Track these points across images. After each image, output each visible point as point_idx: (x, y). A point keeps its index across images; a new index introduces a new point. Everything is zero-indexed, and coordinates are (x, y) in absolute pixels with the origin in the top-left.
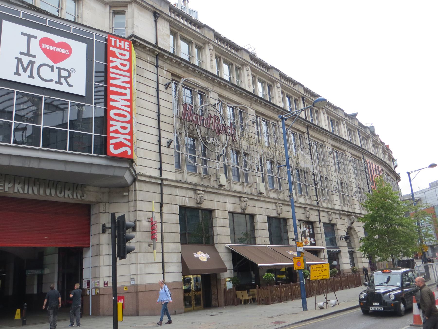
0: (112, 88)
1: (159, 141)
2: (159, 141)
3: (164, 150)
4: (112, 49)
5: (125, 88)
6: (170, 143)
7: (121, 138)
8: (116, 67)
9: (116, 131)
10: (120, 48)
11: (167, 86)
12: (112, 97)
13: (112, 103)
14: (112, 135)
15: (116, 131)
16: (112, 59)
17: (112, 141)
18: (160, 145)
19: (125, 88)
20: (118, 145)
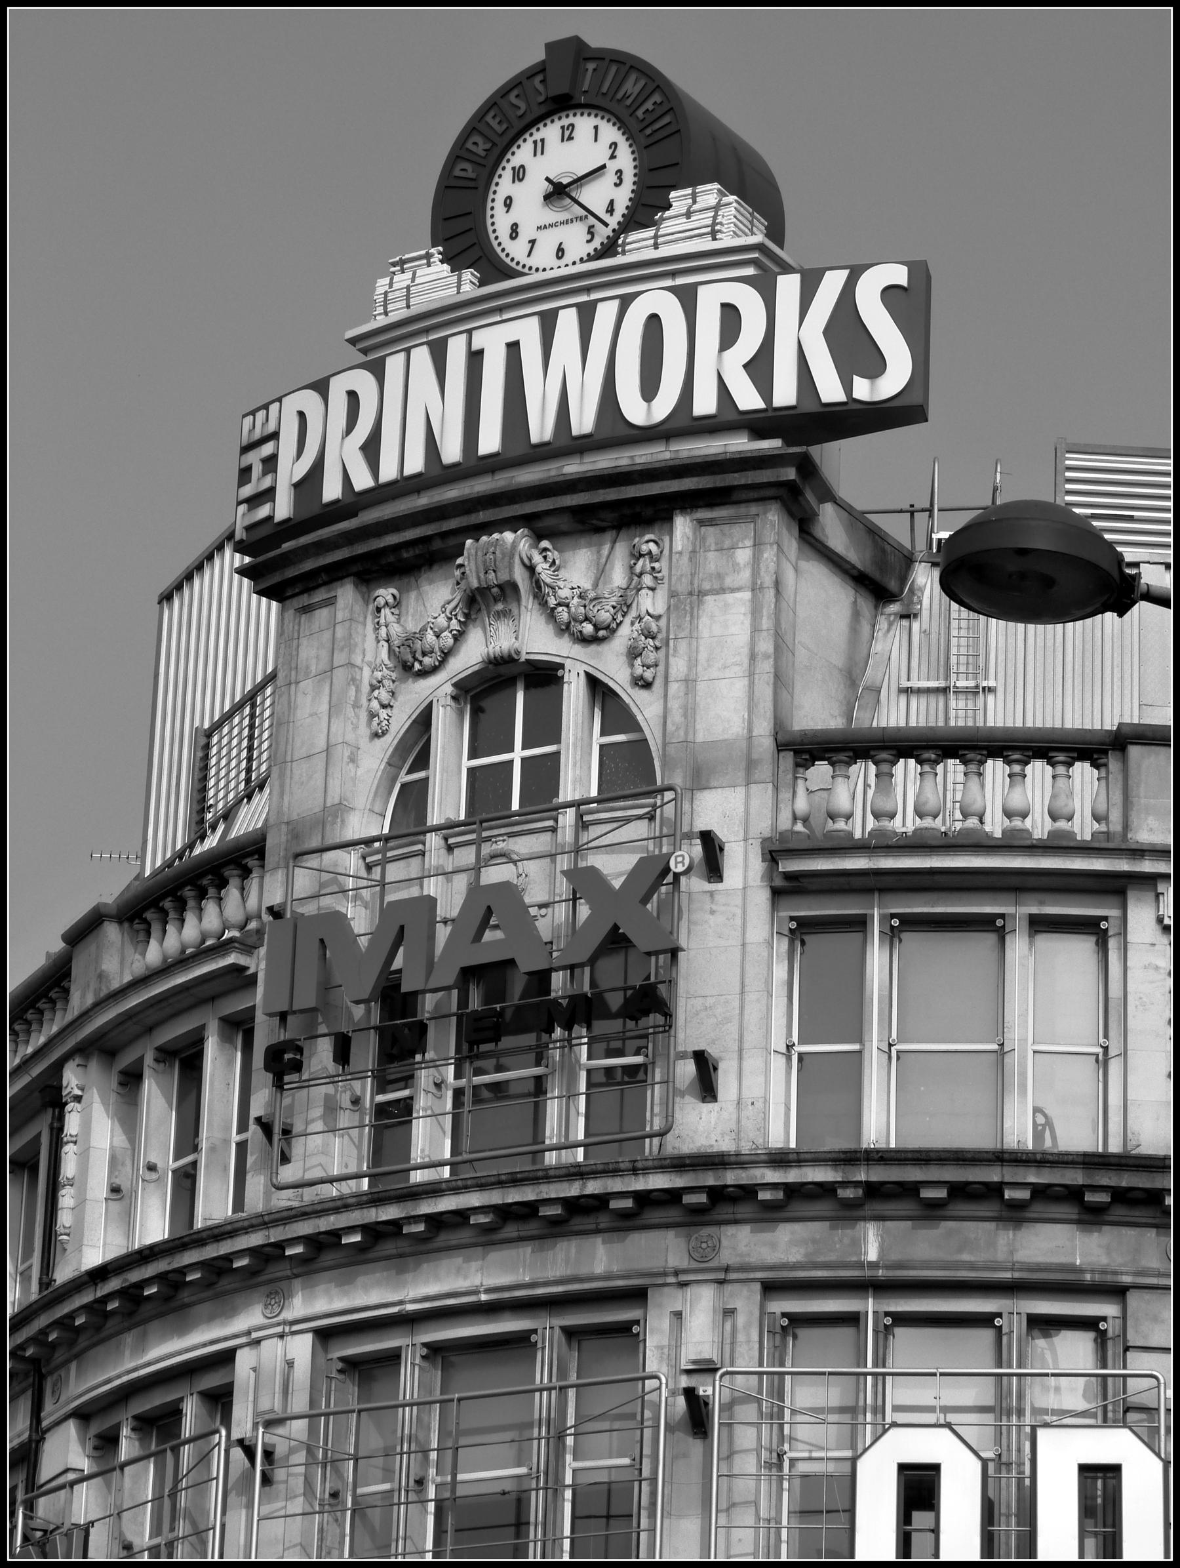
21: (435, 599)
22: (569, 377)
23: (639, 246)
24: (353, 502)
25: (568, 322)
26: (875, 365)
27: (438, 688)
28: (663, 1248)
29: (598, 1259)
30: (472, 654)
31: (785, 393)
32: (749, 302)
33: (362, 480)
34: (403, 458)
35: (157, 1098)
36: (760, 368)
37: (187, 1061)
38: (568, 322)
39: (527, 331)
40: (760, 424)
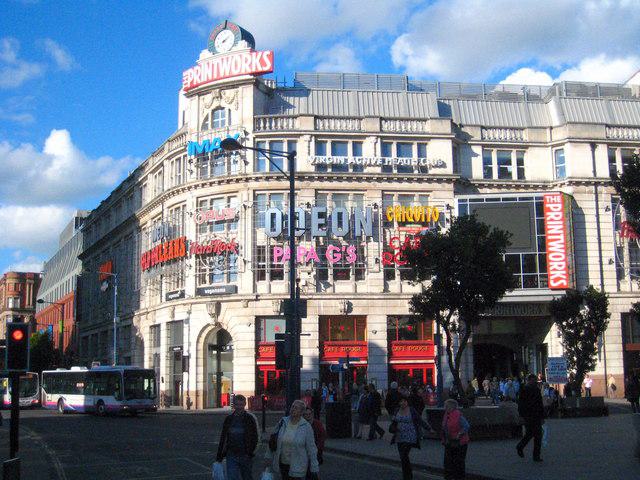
0: (550, 237)
1: (601, 261)
2: (601, 261)
3: (605, 268)
4: (547, 205)
5: (559, 234)
6: (611, 262)
7: (558, 274)
8: (552, 220)
9: (555, 270)
10: (554, 202)
11: (607, 209)
12: (550, 244)
13: (550, 249)
14: (552, 273)
15: (555, 270)
16: (548, 213)
17: (552, 277)
18: (601, 265)
19: (559, 234)
20: (556, 280)
21: (208, 98)
22: (225, 69)
23: (234, 49)
24: (197, 86)
25: (225, 61)
26: (265, 65)
27: (209, 111)
28: (241, 185)
29: (233, 186)
30: (213, 107)
31: (254, 70)
32: (249, 57)
33: (199, 82)
34: (204, 79)
35: (176, 164)
36: (250, 66)
37: (179, 159)
38: (225, 61)
39: (220, 63)
40: (251, 74)
